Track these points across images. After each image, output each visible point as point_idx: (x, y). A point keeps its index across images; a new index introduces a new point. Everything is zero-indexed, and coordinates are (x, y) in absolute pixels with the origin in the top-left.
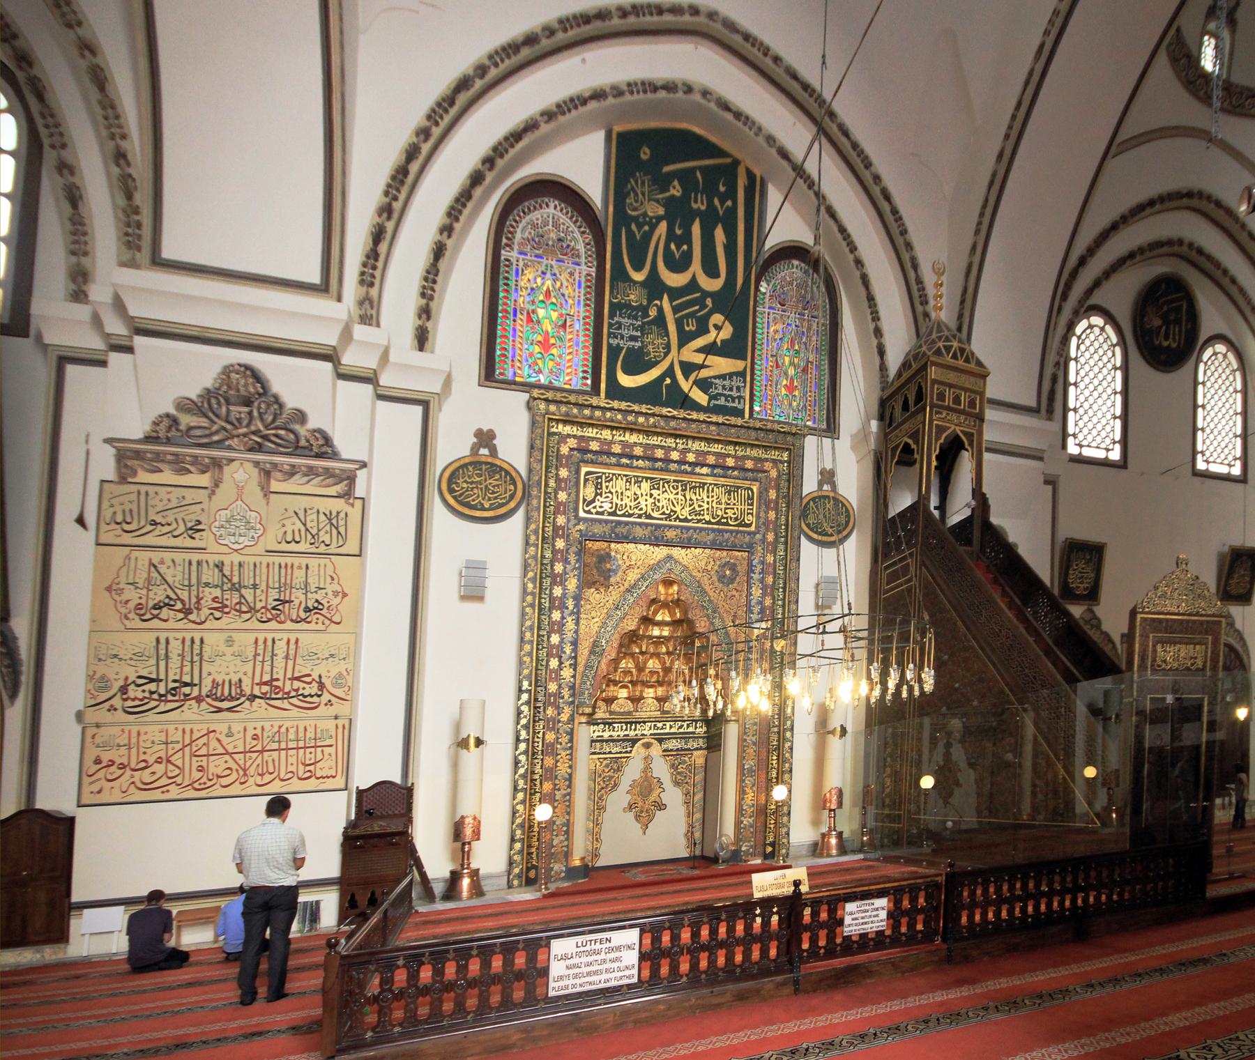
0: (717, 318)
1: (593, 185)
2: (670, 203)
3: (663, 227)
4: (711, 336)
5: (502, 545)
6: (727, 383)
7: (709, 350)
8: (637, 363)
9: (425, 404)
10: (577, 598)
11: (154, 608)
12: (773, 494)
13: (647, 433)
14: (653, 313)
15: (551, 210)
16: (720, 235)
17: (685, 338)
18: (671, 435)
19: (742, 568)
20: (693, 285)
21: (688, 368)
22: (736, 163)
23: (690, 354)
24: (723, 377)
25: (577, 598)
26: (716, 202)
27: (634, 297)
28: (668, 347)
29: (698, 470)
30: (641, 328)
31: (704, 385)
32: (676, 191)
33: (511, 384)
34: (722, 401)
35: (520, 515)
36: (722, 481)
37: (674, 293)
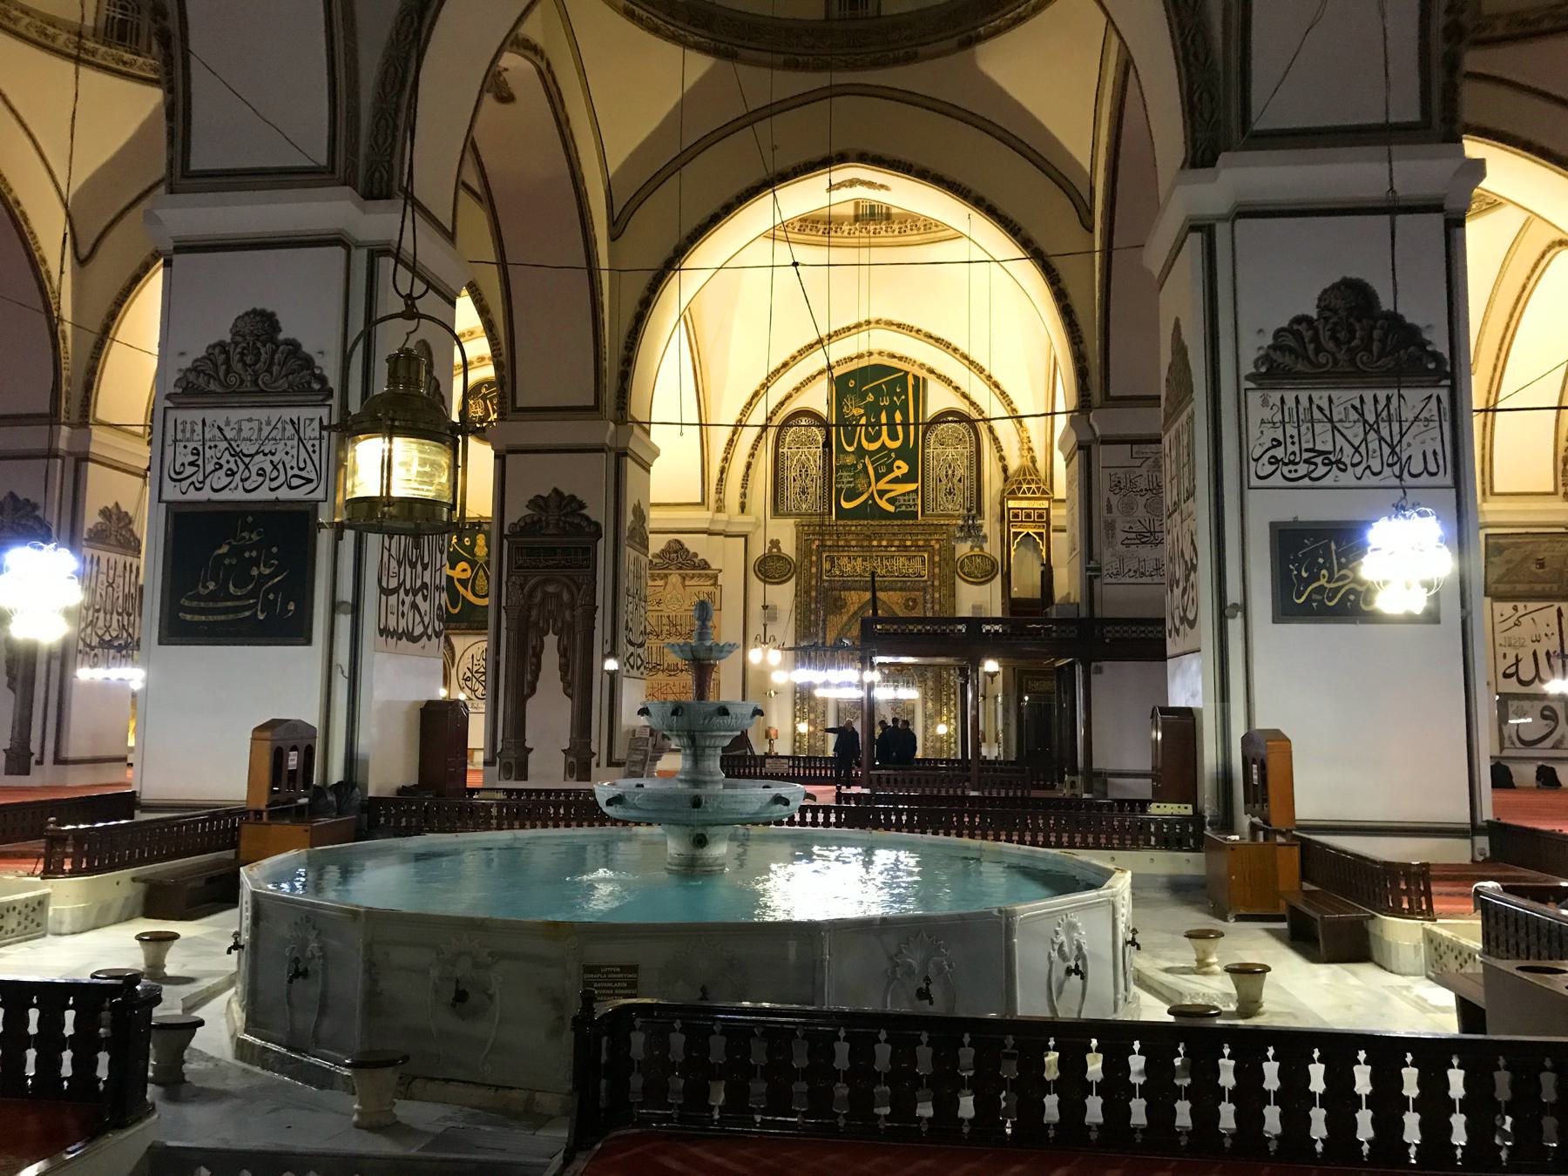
0: (899, 463)
1: (823, 409)
2: (865, 407)
3: (863, 421)
4: (898, 473)
5: (784, 595)
7: (896, 480)
8: (852, 495)
9: (746, 536)
10: (824, 621)
11: (644, 633)
12: (937, 559)
17: (879, 478)
19: (920, 601)
20: (883, 446)
21: (882, 493)
22: (907, 373)
23: (882, 485)
25: (824, 621)
27: (850, 460)
31: (891, 501)
32: (870, 398)
33: (789, 515)
35: (793, 580)
37: (872, 454)
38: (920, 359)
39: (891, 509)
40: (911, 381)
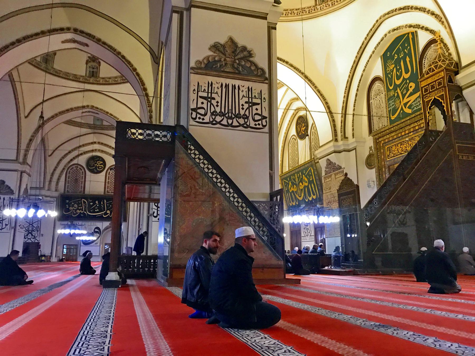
6: (416, 102)
7: (411, 94)
13: (395, 131)
14: (396, 95)
15: (377, 84)
16: (408, 59)
18: (400, 129)
21: (405, 105)
24: (414, 101)
26: (406, 50)
27: (392, 93)
28: (400, 102)
29: (410, 134)
30: (394, 101)
31: (409, 108)
34: (415, 108)
36: (416, 135)
37: (399, 86)
38: (404, 23)
39: (409, 111)
40: (411, 36)
